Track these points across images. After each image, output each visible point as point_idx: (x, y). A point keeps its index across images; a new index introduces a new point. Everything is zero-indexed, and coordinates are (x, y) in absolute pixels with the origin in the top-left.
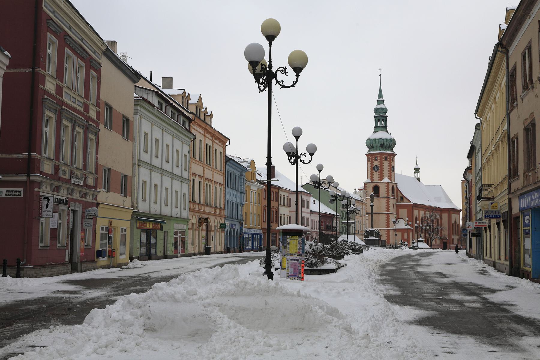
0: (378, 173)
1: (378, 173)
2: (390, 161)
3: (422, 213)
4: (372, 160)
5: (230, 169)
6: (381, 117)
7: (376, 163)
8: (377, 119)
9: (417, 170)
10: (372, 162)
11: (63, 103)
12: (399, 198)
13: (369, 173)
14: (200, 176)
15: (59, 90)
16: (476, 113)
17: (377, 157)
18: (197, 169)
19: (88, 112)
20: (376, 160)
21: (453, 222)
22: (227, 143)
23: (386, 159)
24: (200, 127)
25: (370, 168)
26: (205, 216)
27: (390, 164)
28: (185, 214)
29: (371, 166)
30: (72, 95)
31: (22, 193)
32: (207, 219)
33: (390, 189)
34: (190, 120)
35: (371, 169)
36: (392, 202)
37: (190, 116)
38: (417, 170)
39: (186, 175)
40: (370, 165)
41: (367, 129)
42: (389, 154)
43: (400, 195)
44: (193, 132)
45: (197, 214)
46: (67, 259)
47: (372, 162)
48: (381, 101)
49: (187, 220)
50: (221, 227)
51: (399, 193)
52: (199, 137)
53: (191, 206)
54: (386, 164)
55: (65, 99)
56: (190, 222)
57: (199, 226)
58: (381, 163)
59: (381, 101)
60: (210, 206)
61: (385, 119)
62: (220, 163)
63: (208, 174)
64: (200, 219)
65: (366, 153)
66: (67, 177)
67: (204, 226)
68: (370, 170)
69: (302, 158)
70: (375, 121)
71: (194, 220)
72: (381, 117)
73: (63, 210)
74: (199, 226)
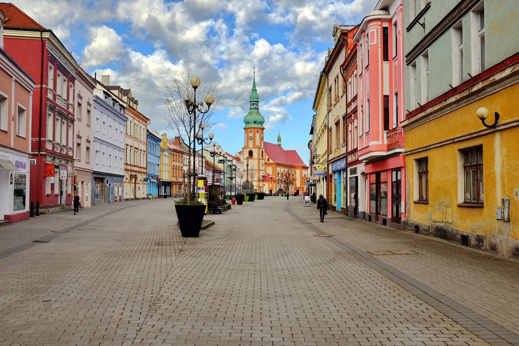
0: (252, 141)
1: (252, 141)
3: (282, 169)
5: (150, 140)
7: (251, 135)
9: (279, 139)
10: (248, 134)
11: (56, 104)
12: (267, 159)
13: (246, 141)
14: (131, 147)
15: (55, 96)
16: (313, 108)
18: (130, 142)
19: (68, 108)
20: (251, 132)
21: (304, 176)
22: (149, 123)
23: (258, 132)
24: (130, 112)
25: (246, 138)
26: (134, 174)
27: (261, 135)
28: (122, 173)
30: (61, 100)
31: (35, 162)
32: (136, 175)
34: (124, 108)
37: (125, 105)
38: (279, 139)
39: (123, 146)
40: (246, 136)
42: (259, 128)
43: (267, 157)
44: (127, 115)
45: (129, 172)
46: (59, 202)
49: (122, 177)
50: (144, 181)
51: (267, 156)
52: (130, 119)
53: (126, 167)
54: (258, 135)
55: (58, 102)
56: (125, 178)
57: (131, 180)
58: (254, 134)
60: (137, 166)
62: (143, 137)
63: (136, 145)
64: (131, 176)
66: (59, 151)
67: (133, 181)
68: (246, 139)
69: (205, 141)
71: (127, 176)
73: (57, 172)
74: (131, 180)
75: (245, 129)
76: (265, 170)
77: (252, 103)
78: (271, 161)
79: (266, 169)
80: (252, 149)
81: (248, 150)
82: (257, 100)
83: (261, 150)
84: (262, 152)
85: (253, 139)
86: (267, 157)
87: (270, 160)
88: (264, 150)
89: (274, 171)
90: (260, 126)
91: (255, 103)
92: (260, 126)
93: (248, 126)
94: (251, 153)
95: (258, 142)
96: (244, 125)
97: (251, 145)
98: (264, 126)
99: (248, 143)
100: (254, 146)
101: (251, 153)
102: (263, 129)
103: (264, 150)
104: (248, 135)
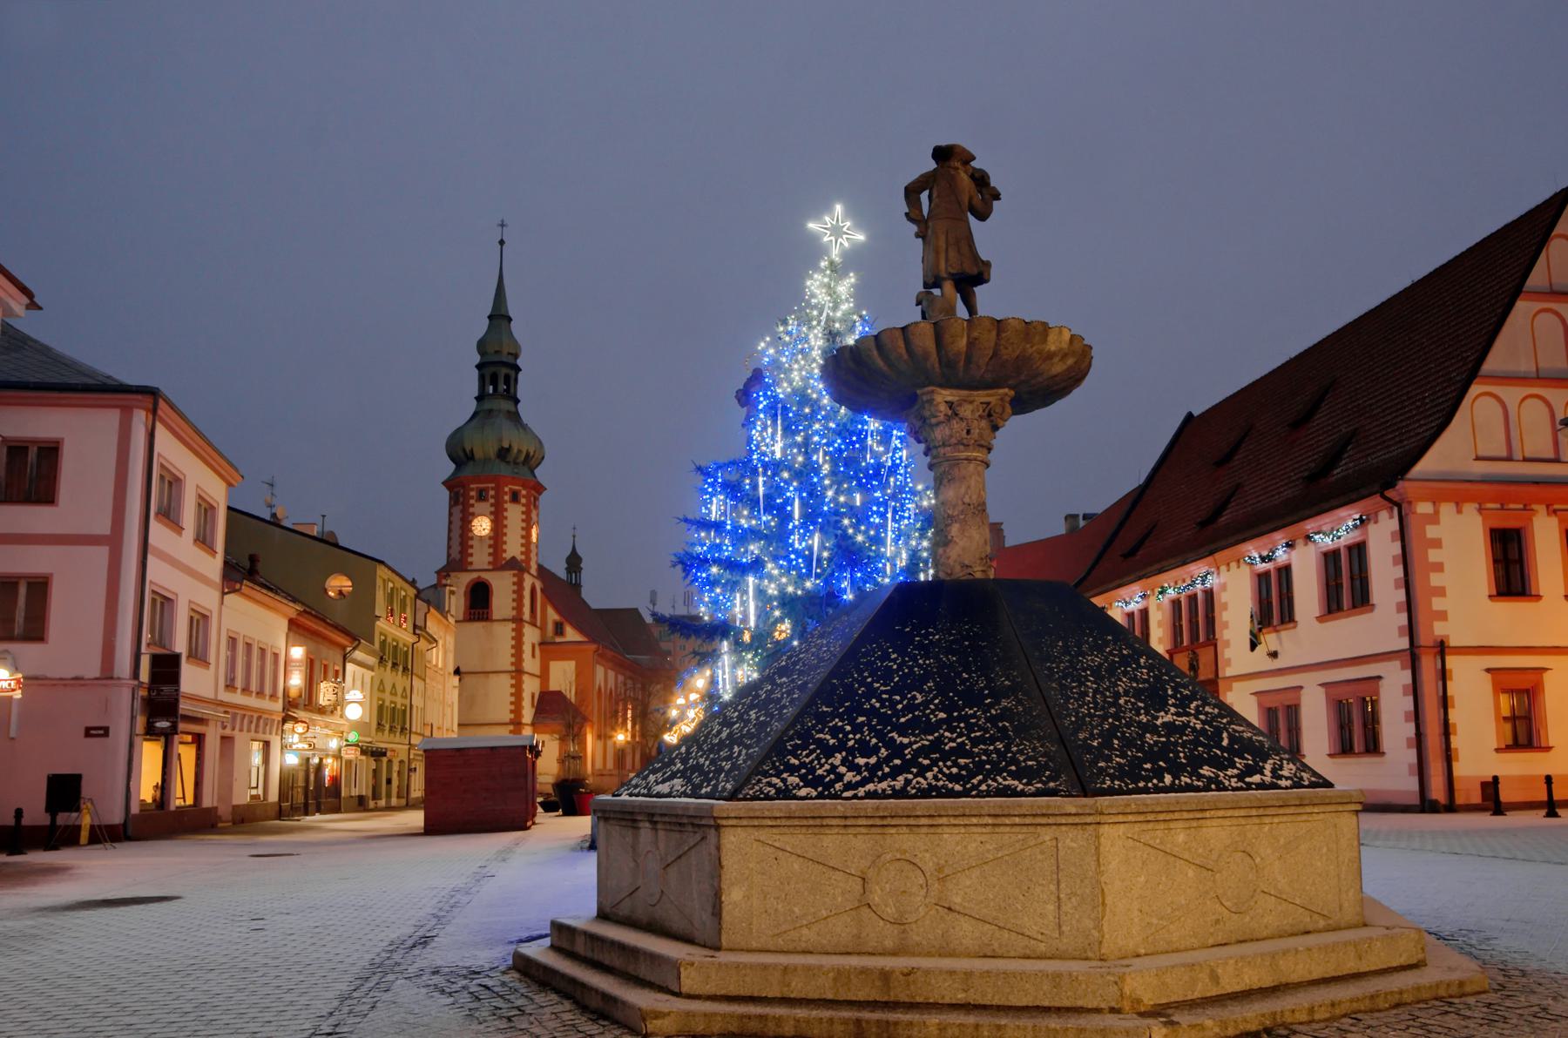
2: (527, 505)
4: (467, 497)
6: (498, 372)
8: (488, 371)
12: (550, 627)
17: (486, 490)
23: (515, 498)
36: (531, 635)
48: (499, 317)
59: (499, 317)
61: (512, 373)
70: (482, 378)
76: (544, 676)
77: (488, 371)
82: (510, 360)
86: (552, 615)
91: (504, 371)
102: (539, 488)
103: (538, 586)
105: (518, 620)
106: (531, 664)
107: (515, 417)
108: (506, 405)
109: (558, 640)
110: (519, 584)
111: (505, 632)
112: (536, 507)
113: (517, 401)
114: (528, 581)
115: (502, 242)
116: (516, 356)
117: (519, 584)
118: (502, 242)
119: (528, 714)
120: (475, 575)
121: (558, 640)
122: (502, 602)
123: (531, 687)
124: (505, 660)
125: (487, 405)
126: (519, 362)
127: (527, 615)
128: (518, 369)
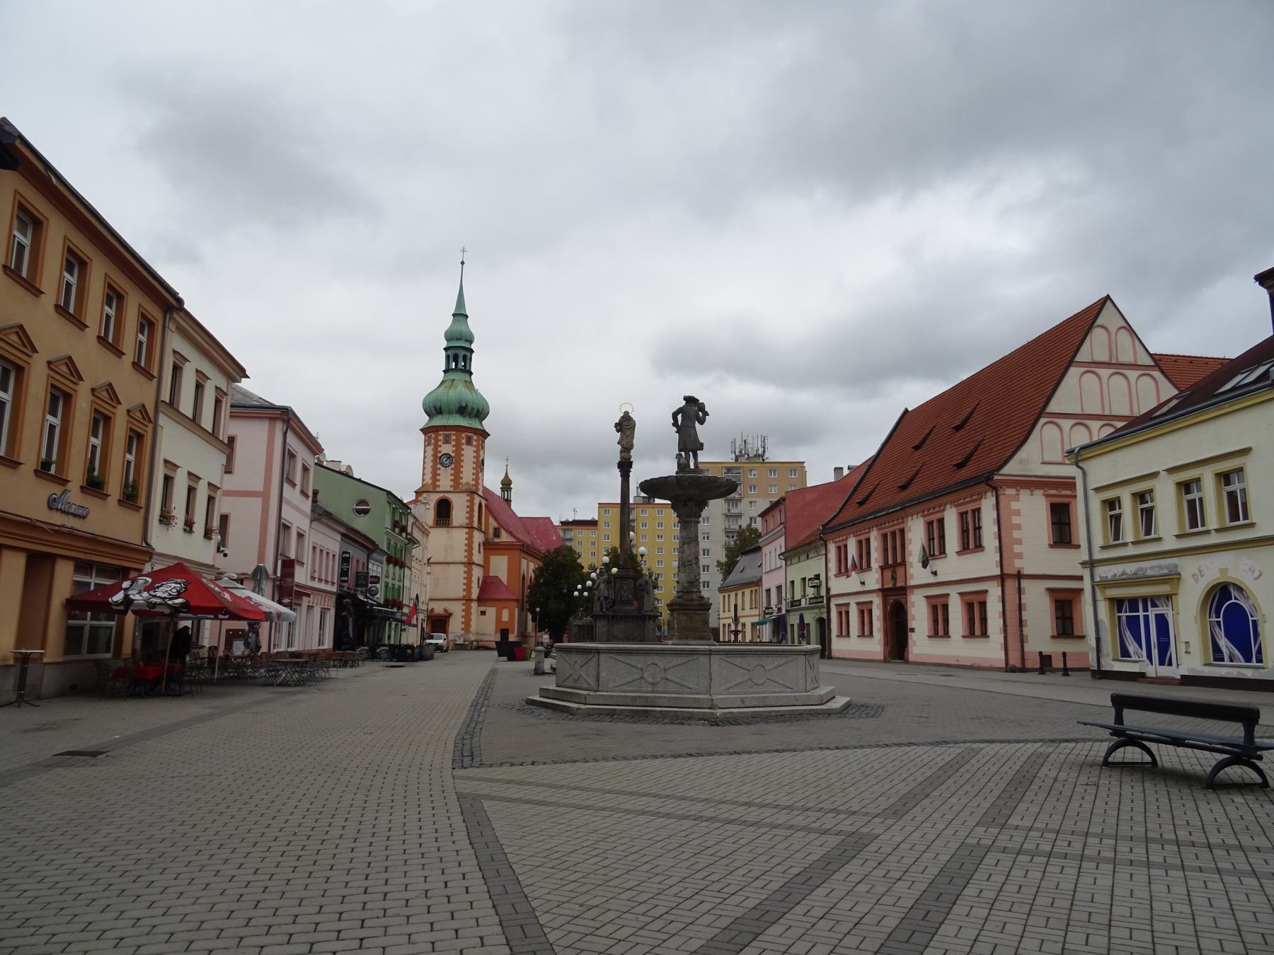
0: (450, 471)
1: (450, 471)
4: (437, 440)
6: (459, 354)
7: (447, 449)
8: (451, 353)
10: (436, 446)
12: (491, 531)
13: (429, 470)
20: (447, 441)
23: (469, 442)
25: (430, 458)
27: (477, 452)
29: (435, 455)
33: (476, 508)
35: (434, 461)
36: (478, 538)
41: (430, 372)
43: (493, 523)
47: (436, 446)
48: (460, 315)
51: (491, 520)
54: (468, 452)
58: (458, 448)
59: (460, 315)
65: (422, 426)
70: (448, 357)
72: (459, 354)
75: (425, 431)
76: (485, 566)
78: (505, 537)
79: (487, 560)
80: (448, 496)
81: (435, 498)
82: (466, 345)
83: (477, 500)
84: (480, 505)
85: (453, 461)
87: (503, 533)
88: (484, 503)
89: (513, 569)
90: (474, 424)
91: (461, 353)
92: (474, 424)
93: (438, 421)
94: (444, 509)
95: (467, 476)
96: (424, 420)
97: (445, 481)
98: (487, 424)
99: (435, 475)
100: (457, 487)
101: (444, 509)
102: (484, 434)
104: (436, 450)
105: (470, 527)
106: (478, 558)
107: (469, 384)
108: (466, 377)
109: (496, 540)
110: (471, 501)
111: (461, 535)
112: (483, 448)
113: (471, 374)
114: (477, 500)
115: (463, 263)
116: (471, 342)
117: (471, 501)
118: (463, 263)
119: (475, 593)
120: (441, 495)
121: (496, 540)
122: (459, 513)
123: (477, 573)
124: (461, 556)
125: (451, 376)
126: (473, 347)
127: (476, 525)
128: (472, 351)
